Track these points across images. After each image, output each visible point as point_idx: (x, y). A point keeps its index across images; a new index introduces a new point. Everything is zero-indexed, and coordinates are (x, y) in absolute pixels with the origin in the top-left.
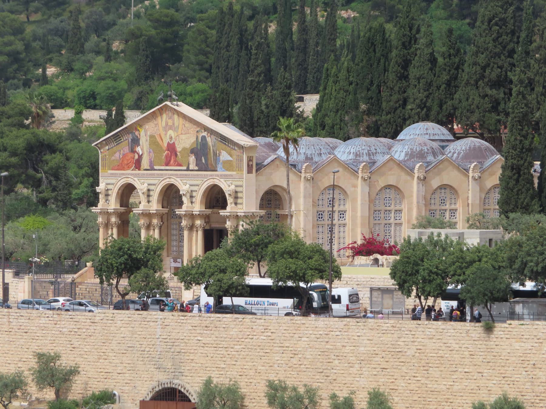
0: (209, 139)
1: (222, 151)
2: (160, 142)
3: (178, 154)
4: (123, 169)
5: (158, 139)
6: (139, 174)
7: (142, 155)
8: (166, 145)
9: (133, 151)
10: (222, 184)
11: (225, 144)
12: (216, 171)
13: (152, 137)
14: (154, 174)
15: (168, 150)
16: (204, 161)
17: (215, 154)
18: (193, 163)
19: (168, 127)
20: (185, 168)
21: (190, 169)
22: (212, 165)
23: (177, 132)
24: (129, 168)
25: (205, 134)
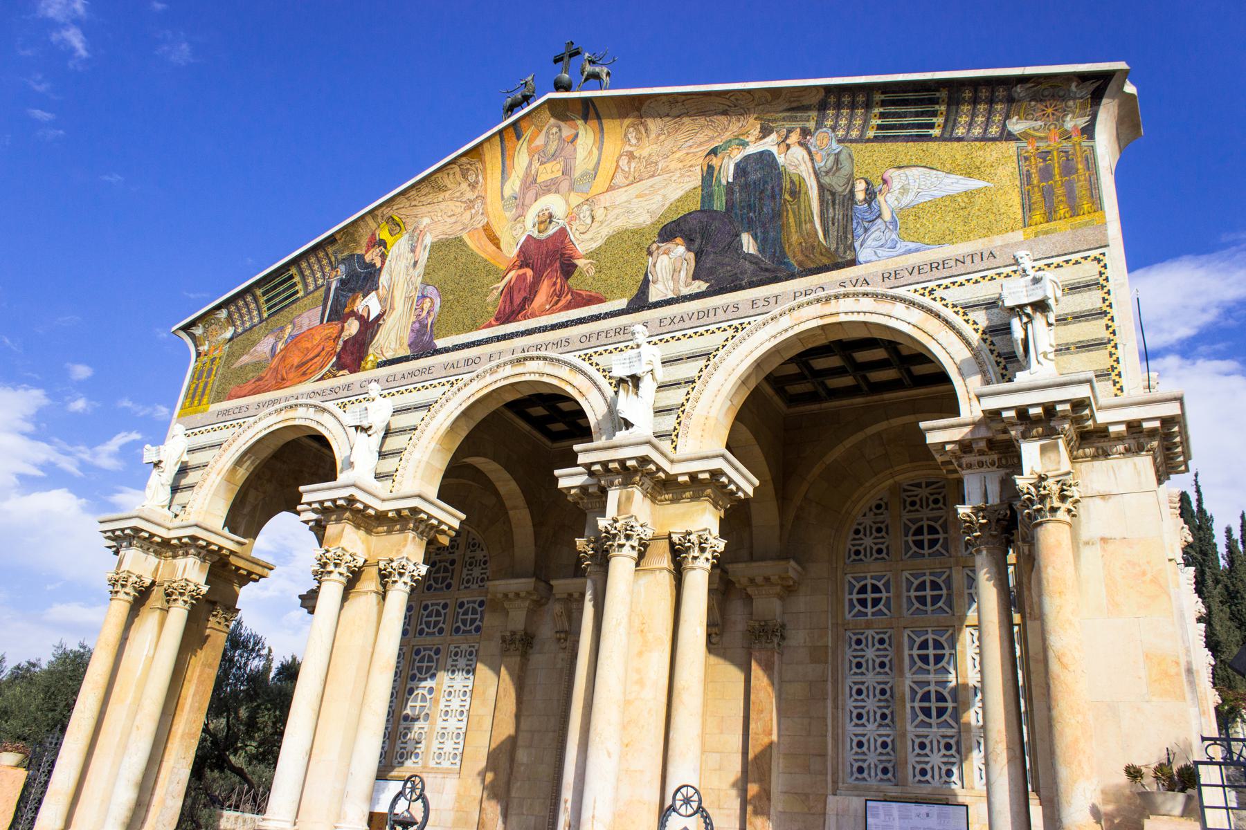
1: (893, 174)
3: (580, 262)
4: (281, 383)
5: (477, 245)
6: (348, 387)
8: (516, 250)
9: (338, 314)
10: (899, 309)
11: (928, 138)
12: (853, 263)
14: (429, 370)
15: (521, 267)
16: (748, 244)
18: (675, 271)
20: (622, 303)
21: (653, 298)
22: (810, 246)
25: (770, 144)
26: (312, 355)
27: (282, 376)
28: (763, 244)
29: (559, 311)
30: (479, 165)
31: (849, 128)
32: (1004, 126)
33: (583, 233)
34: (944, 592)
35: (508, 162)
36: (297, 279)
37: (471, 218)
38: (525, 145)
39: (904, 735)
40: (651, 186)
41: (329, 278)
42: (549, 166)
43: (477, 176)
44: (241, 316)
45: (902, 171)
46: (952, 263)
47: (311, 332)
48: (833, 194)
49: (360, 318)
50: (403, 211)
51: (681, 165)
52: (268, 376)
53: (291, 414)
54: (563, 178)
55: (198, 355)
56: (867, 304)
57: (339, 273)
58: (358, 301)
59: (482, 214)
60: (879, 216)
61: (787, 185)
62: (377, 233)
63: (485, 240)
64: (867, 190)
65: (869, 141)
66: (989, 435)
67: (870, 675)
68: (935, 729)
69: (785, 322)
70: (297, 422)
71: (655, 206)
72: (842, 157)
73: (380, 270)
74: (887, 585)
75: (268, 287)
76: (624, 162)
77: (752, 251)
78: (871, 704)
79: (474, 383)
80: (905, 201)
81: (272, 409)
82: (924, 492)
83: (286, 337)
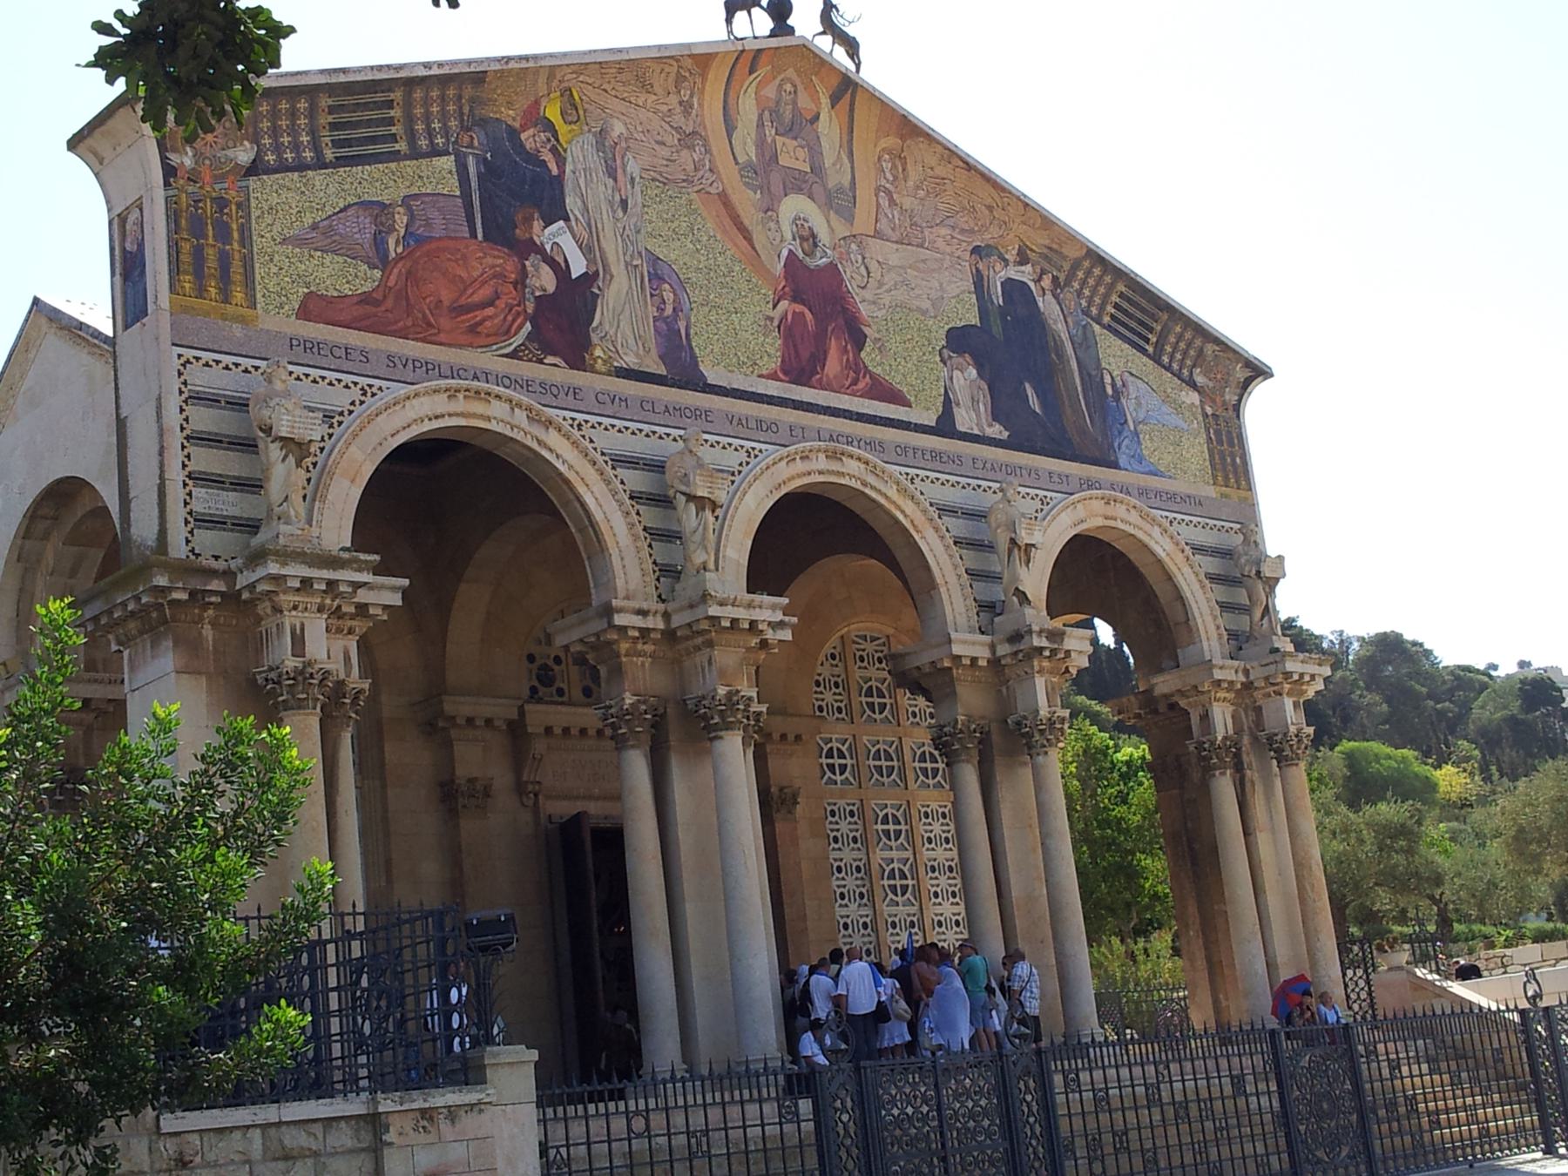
0: (1047, 305)
4: (425, 332)
6: (575, 392)
7: (589, 278)
8: (779, 268)
10: (1156, 531)
12: (1115, 465)
15: (795, 299)
17: (1093, 380)
20: (930, 419)
24: (475, 336)
26: (476, 298)
27: (424, 315)
28: (1043, 404)
29: (861, 396)
30: (699, 80)
31: (1090, 302)
32: (1191, 373)
33: (863, 288)
34: (895, 763)
35: (731, 101)
36: (395, 113)
37: (696, 169)
38: (754, 84)
39: (882, 914)
40: (924, 261)
41: (456, 142)
42: (792, 143)
43: (691, 96)
44: (275, 132)
45: (1132, 379)
46: (1179, 500)
47: (451, 244)
48: (1090, 375)
49: (551, 262)
50: (588, 90)
51: (948, 249)
52: (390, 303)
53: (478, 407)
54: (811, 178)
55: (169, 172)
56: (1134, 517)
57: (476, 143)
58: (537, 225)
59: (711, 170)
60: (1126, 421)
61: (1050, 339)
62: (544, 104)
63: (727, 221)
64: (1113, 385)
65: (1103, 326)
66: (1244, 680)
67: (846, 850)
68: (901, 908)
69: (1081, 511)
70: (493, 426)
71: (934, 295)
72: (1089, 335)
73: (560, 179)
74: (850, 748)
75: (349, 100)
76: (884, 202)
77: (1037, 410)
78: (851, 883)
79: (784, 463)
80: (1141, 416)
81: (443, 383)
82: (870, 647)
83: (402, 234)
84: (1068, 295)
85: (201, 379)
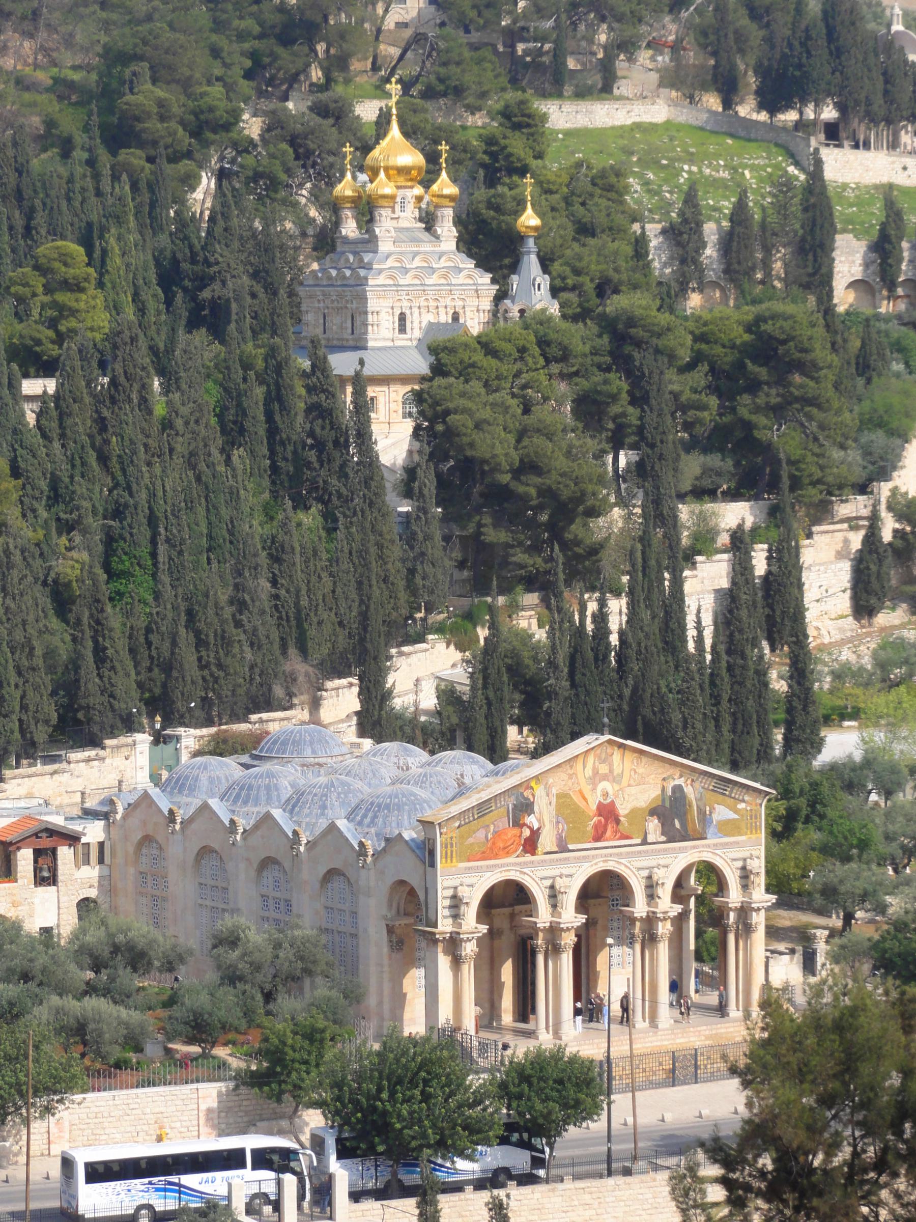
0: (689, 790)
2: (582, 804)
3: (622, 819)
4: (496, 857)
5: (576, 798)
6: (532, 862)
7: (539, 829)
9: (518, 823)
13: (563, 797)
14: (567, 859)
15: (600, 815)
16: (677, 824)
17: (702, 812)
19: (596, 778)
20: (639, 841)
22: (695, 830)
23: (619, 783)
24: (508, 854)
28: (681, 824)
49: (529, 827)
80: (720, 818)
84: (697, 785)
85: (446, 884)
